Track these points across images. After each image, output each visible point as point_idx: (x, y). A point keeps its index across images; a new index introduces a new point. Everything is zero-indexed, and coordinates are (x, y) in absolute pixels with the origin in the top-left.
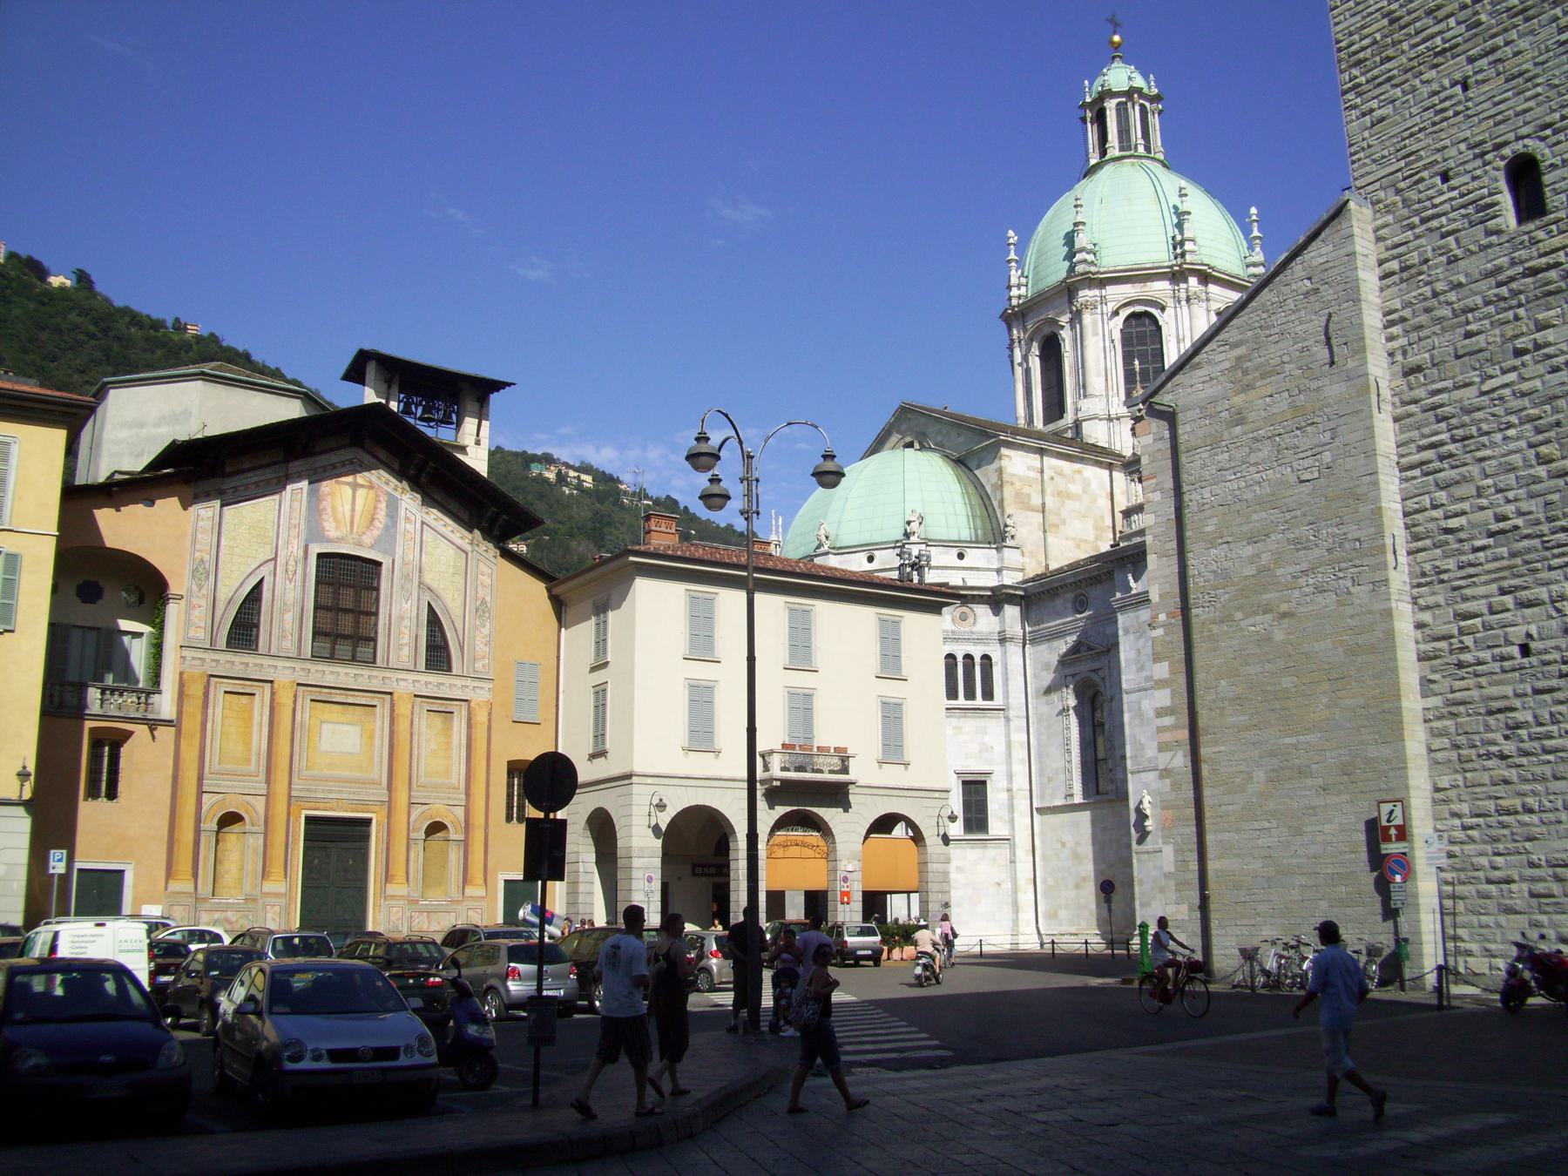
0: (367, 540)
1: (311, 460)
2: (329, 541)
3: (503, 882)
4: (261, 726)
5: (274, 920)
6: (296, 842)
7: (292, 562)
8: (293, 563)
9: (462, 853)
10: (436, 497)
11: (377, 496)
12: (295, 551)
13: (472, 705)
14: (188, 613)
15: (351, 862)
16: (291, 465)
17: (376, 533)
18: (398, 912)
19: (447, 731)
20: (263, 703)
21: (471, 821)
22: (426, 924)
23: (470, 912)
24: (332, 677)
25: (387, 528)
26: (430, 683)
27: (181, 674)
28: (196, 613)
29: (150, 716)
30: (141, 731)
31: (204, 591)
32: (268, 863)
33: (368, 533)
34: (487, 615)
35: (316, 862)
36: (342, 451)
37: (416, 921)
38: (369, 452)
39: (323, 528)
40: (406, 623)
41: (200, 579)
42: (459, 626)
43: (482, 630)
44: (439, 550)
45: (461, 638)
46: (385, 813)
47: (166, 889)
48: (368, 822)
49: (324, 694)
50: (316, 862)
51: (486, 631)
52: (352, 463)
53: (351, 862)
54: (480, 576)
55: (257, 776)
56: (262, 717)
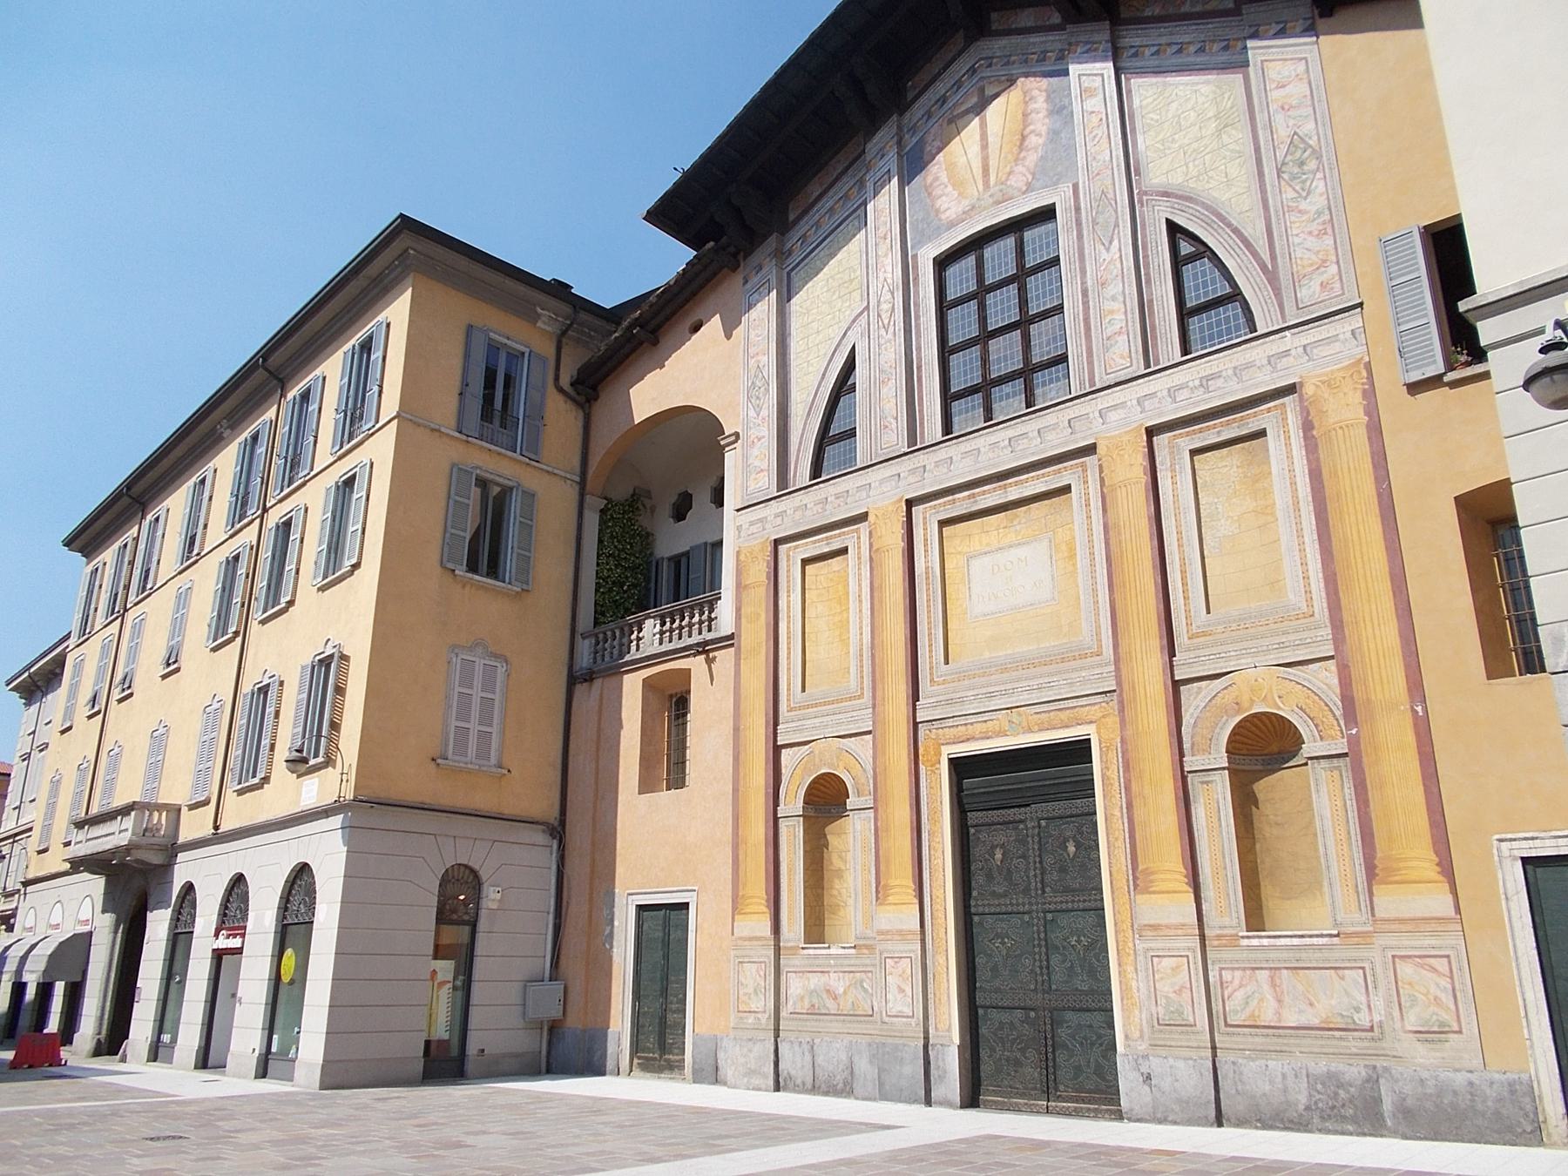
0: (1018, 181)
1: (908, 115)
2: (952, 225)
3: (1520, 862)
4: (860, 601)
5: (901, 990)
6: (935, 813)
7: (887, 296)
8: (889, 296)
9: (1349, 791)
10: (1148, 13)
11: (1025, 93)
12: (890, 275)
13: (1309, 390)
14: (745, 457)
15: (1072, 849)
16: (869, 146)
17: (1032, 158)
18: (1175, 969)
19: (1257, 481)
20: (859, 558)
21: (1358, 693)
22: (1270, 1004)
23: (1406, 970)
24: (969, 461)
25: (1054, 134)
26: (1181, 387)
27: (738, 553)
28: (755, 452)
29: (710, 636)
30: (696, 664)
31: (764, 413)
32: (882, 868)
33: (1020, 168)
34: (1312, 165)
35: (999, 856)
36: (954, 67)
37: (1240, 995)
38: (1009, 32)
39: (937, 211)
40: (1115, 288)
41: (758, 398)
42: (1255, 232)
43: (1303, 205)
44: (1174, 105)
45: (1266, 257)
46: (1113, 721)
47: (733, 934)
48: (1079, 751)
49: (961, 504)
50: (999, 856)
51: (1316, 202)
52: (975, 71)
53: (1072, 849)
54: (1275, 95)
55: (861, 696)
56: (860, 585)
